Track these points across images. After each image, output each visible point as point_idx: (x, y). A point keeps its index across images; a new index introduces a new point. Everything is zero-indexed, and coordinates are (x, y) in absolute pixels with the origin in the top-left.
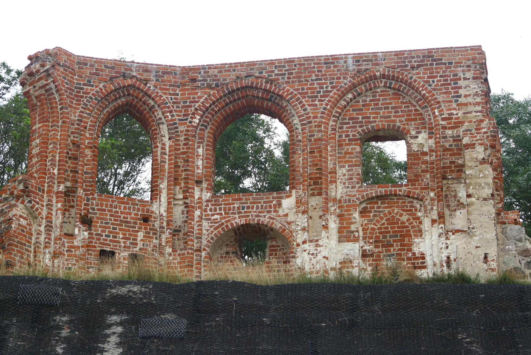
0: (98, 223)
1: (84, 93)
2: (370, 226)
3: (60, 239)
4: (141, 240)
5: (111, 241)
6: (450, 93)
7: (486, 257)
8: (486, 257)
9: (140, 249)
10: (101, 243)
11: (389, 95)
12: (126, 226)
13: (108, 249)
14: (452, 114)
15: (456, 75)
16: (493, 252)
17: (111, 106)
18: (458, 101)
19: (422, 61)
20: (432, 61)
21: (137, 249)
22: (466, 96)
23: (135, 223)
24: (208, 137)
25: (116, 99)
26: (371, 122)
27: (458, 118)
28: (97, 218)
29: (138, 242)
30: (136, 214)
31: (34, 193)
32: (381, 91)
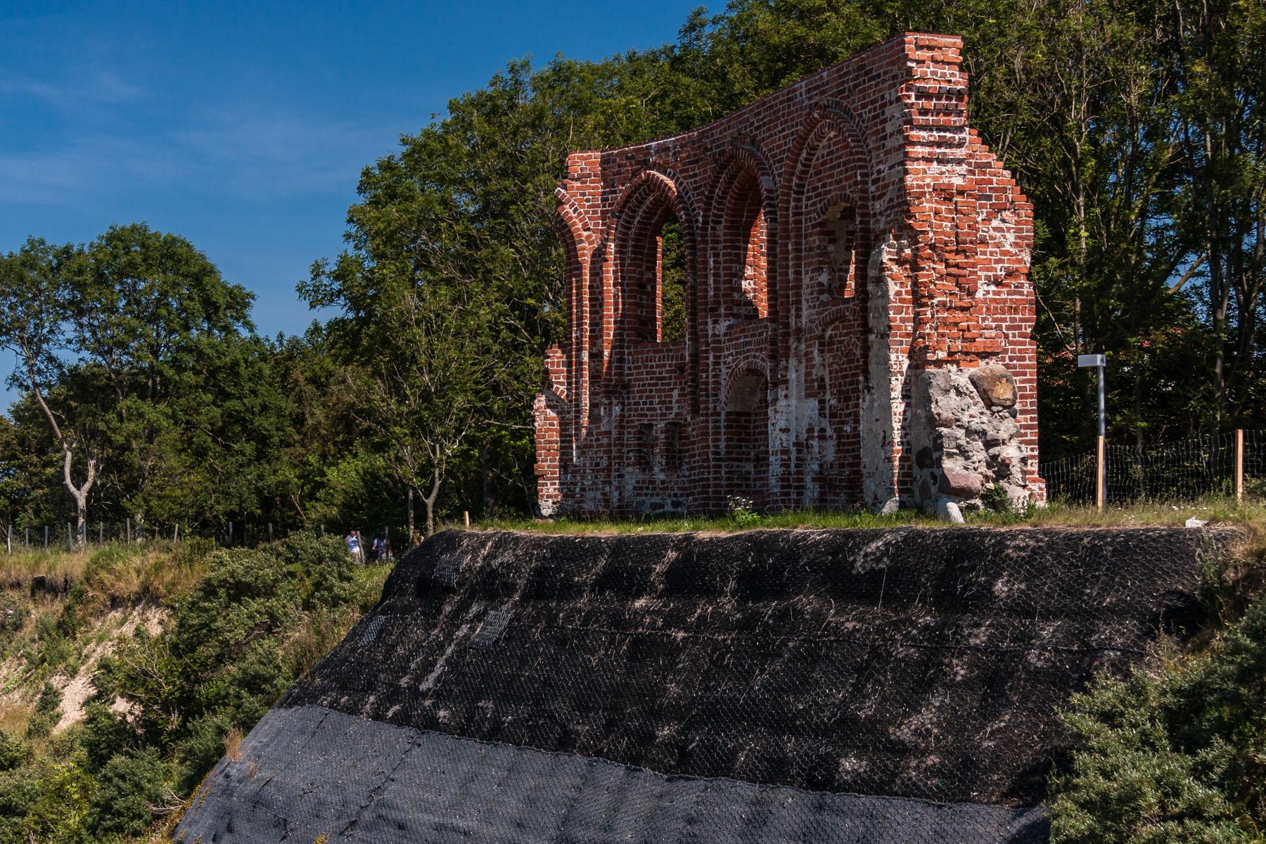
2: (835, 367)
4: (677, 402)
5: (649, 409)
6: (876, 132)
8: (884, 437)
9: (677, 414)
14: (879, 172)
15: (883, 97)
17: (640, 212)
19: (857, 77)
20: (867, 73)
21: (672, 416)
22: (892, 135)
23: (670, 378)
24: (725, 234)
26: (827, 193)
27: (884, 179)
28: (636, 380)
30: (671, 365)
31: (555, 372)
32: (835, 136)
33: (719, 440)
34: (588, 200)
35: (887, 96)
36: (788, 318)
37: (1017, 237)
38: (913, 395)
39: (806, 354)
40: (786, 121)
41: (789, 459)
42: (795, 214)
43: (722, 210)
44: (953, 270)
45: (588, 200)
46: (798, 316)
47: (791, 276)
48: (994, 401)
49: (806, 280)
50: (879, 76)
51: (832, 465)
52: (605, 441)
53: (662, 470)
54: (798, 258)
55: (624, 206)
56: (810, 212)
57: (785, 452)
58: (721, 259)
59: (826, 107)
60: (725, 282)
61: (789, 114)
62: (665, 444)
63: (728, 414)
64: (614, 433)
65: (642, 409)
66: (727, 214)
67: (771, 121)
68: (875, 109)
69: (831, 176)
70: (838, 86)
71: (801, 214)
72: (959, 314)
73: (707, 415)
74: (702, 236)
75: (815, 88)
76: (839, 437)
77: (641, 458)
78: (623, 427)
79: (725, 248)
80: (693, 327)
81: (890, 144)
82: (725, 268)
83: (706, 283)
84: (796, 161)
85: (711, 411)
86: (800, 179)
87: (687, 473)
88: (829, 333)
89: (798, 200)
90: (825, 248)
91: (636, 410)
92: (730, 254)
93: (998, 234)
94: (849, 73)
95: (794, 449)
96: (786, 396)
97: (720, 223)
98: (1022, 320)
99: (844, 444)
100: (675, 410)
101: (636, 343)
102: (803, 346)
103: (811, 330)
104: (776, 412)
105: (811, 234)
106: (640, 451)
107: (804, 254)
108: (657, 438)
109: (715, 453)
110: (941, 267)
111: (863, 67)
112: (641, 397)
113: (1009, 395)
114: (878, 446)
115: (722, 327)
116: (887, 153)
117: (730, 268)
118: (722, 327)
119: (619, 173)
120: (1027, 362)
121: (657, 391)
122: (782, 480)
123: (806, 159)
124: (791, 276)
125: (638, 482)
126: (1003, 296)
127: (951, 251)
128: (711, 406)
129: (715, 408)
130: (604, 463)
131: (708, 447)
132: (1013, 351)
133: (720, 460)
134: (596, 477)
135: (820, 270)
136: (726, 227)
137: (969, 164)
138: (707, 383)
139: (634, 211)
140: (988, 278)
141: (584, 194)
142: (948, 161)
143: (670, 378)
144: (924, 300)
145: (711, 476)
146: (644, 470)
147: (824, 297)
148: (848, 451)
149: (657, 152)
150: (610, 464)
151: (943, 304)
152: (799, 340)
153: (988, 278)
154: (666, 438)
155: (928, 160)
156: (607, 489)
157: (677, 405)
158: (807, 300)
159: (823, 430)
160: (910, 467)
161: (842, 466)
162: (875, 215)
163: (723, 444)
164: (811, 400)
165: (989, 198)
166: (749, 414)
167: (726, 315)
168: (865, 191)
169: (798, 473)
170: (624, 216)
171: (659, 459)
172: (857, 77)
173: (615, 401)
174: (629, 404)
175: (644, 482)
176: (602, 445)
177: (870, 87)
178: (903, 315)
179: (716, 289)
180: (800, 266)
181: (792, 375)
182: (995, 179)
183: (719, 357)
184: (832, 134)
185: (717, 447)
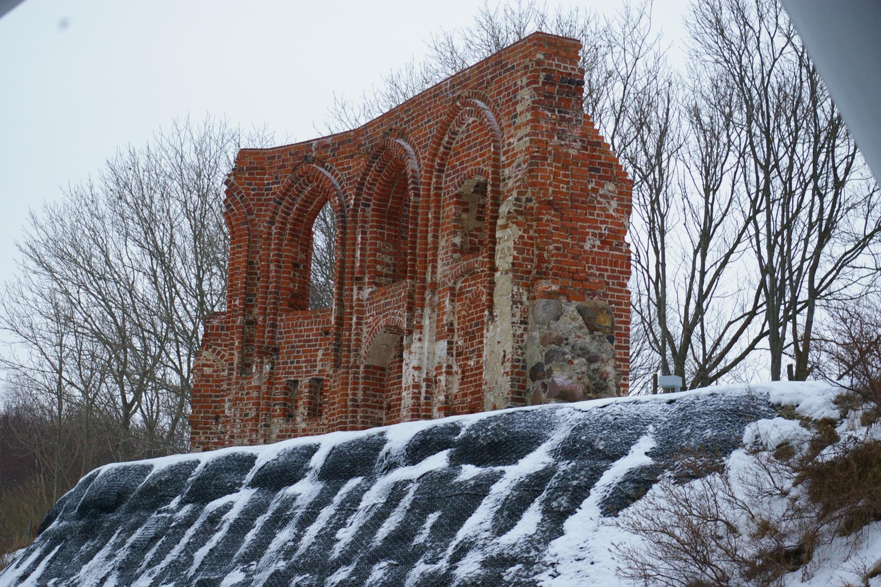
0: (284, 348)
1: (272, 194)
2: (464, 313)
3: (237, 383)
4: (321, 360)
5: (295, 368)
6: (509, 113)
7: (504, 356)
8: (504, 356)
9: (320, 371)
10: (286, 373)
11: (476, 127)
12: (309, 346)
13: (292, 379)
14: (509, 144)
15: (515, 84)
16: (508, 346)
17: (299, 200)
18: (515, 122)
19: (495, 71)
20: (502, 67)
21: (317, 372)
22: (521, 113)
23: (316, 340)
24: (373, 216)
25: (300, 192)
26: (463, 169)
27: (513, 149)
29: (318, 363)
30: (317, 329)
32: (474, 122)
33: (357, 389)
34: (253, 190)
35: (519, 83)
36: (425, 274)
37: (619, 205)
38: (530, 321)
39: (439, 304)
40: (432, 113)
41: (420, 393)
42: (436, 188)
43: (371, 195)
44: (567, 223)
45: (253, 190)
46: (434, 273)
47: (430, 239)
48: (597, 326)
49: (442, 243)
50: (513, 67)
51: (456, 397)
52: (255, 394)
53: (304, 420)
54: (437, 225)
55: (285, 194)
56: (448, 187)
57: (417, 386)
58: (368, 236)
59: (466, 97)
60: (370, 256)
61: (434, 108)
62: (308, 397)
63: (366, 367)
64: (264, 388)
65: (289, 368)
66: (375, 199)
67: (418, 116)
68: (509, 95)
69: (469, 155)
70: (477, 80)
71: (441, 189)
73: (348, 367)
74: (353, 216)
75: (458, 84)
76: (463, 372)
77: (285, 410)
78: (272, 384)
79: (372, 227)
80: (340, 295)
81: (518, 121)
82: (371, 244)
83: (354, 256)
84: (439, 144)
85: (351, 365)
86: (442, 159)
87: (326, 422)
88: (459, 285)
89: (439, 177)
90: (460, 215)
91: (284, 368)
92: (376, 232)
93: (603, 201)
94: (488, 68)
95: (424, 384)
96: (420, 340)
97: (369, 206)
99: (468, 377)
100: (319, 368)
101: (287, 311)
102: (437, 298)
103: (444, 283)
104: (411, 353)
105: (448, 205)
106: (285, 404)
107: (441, 221)
108: (301, 392)
109: (354, 400)
111: (500, 62)
112: (289, 358)
114: (499, 364)
115: (367, 292)
116: (519, 127)
117: (375, 244)
118: (367, 292)
119: (283, 166)
121: (304, 352)
122: (412, 410)
123: (448, 143)
124: (430, 239)
125: (281, 431)
126: (606, 251)
128: (352, 360)
129: (355, 361)
130: (253, 414)
131: (347, 395)
132: (612, 296)
133: (358, 406)
134: (245, 426)
135: (455, 233)
136: (373, 210)
137: (583, 142)
138: (349, 340)
139: (294, 199)
141: (250, 184)
143: (316, 340)
145: (349, 420)
146: (288, 421)
147: (456, 256)
148: (471, 382)
149: (317, 149)
150: (258, 415)
152: (433, 292)
154: (310, 392)
156: (254, 436)
157: (323, 365)
158: (442, 260)
159: (450, 367)
160: (525, 381)
161: (465, 395)
162: (504, 180)
163: (360, 393)
164: (442, 341)
165: (598, 170)
166: (383, 369)
167: (369, 283)
168: (497, 160)
169: (427, 404)
170: (284, 203)
171: (302, 410)
172: (495, 71)
173: (266, 361)
174: (278, 363)
175: (287, 431)
176: (252, 398)
177: (505, 78)
179: (362, 261)
180: (436, 231)
181: (426, 322)
182: (603, 156)
183: (361, 319)
184: (471, 120)
185: (354, 394)
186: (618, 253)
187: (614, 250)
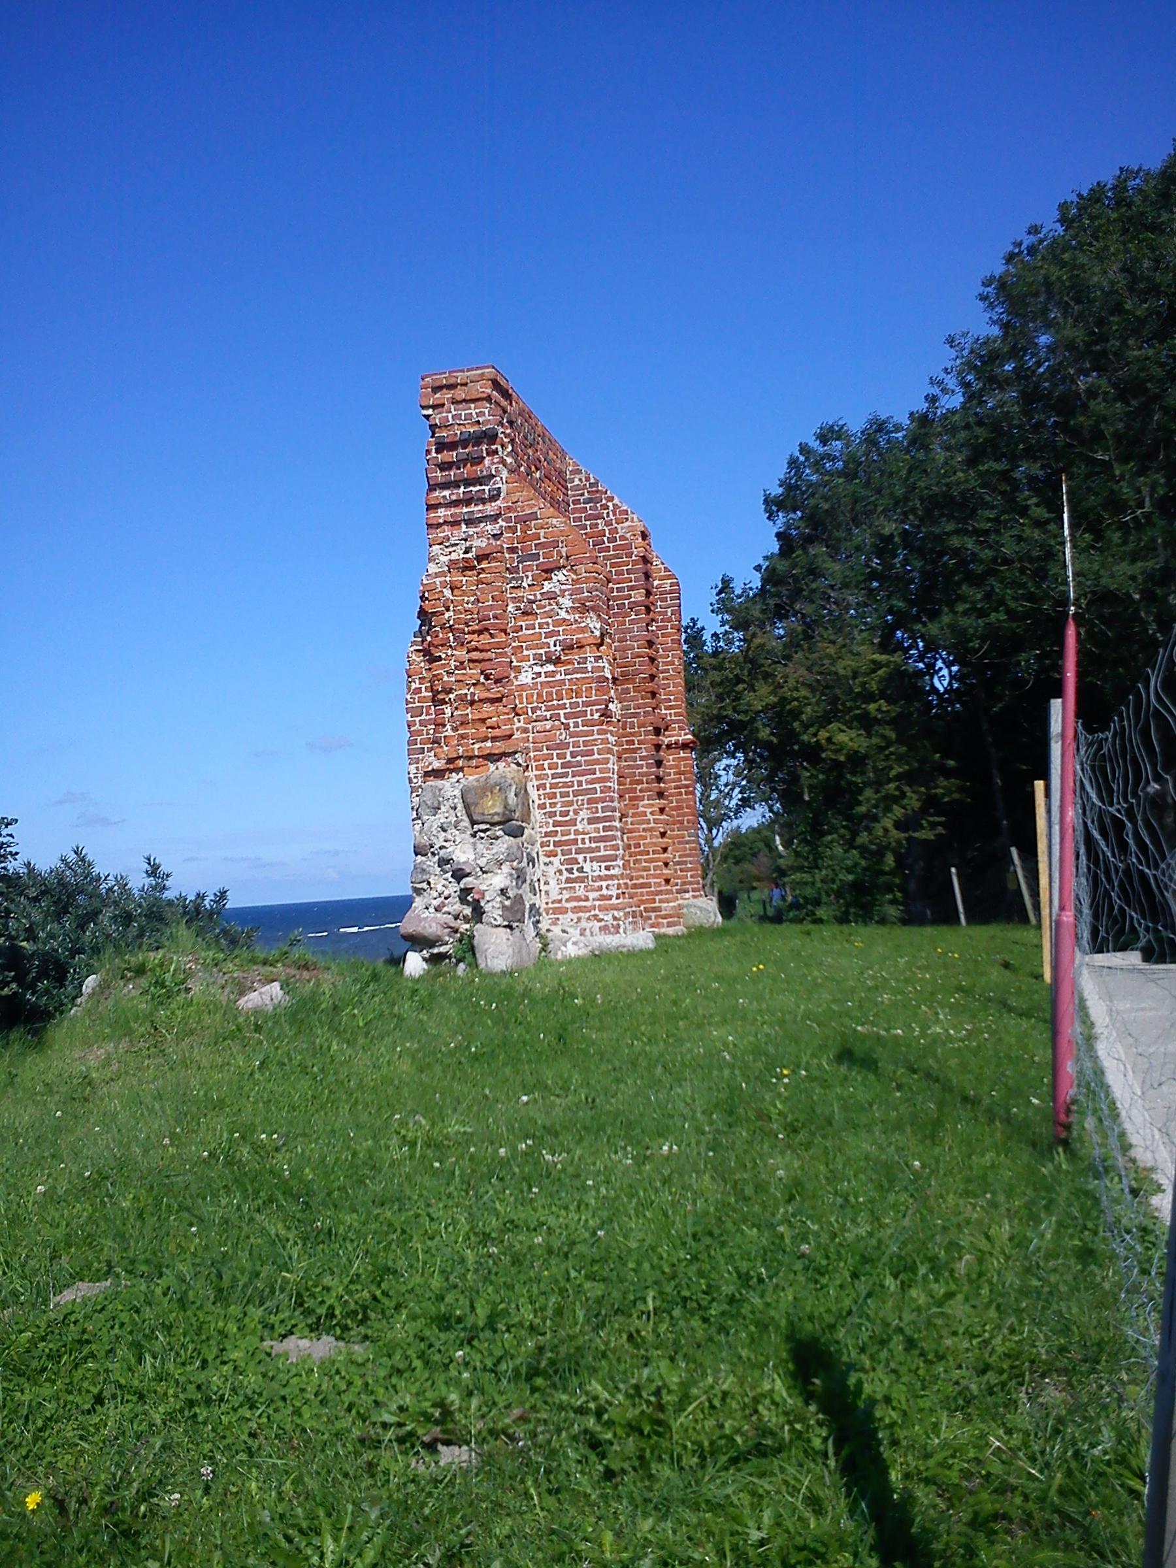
44: (475, 655)
72: (487, 708)
98: (586, 704)
110: (461, 654)
113: (499, 809)
120: (596, 756)
126: (558, 677)
127: (473, 632)
132: (576, 745)
137: (508, 520)
140: (537, 657)
142: (480, 520)
144: (440, 696)
151: (462, 698)
153: (537, 657)
155: (455, 524)
178: (423, 717)
186: (579, 676)
187: (575, 671)
